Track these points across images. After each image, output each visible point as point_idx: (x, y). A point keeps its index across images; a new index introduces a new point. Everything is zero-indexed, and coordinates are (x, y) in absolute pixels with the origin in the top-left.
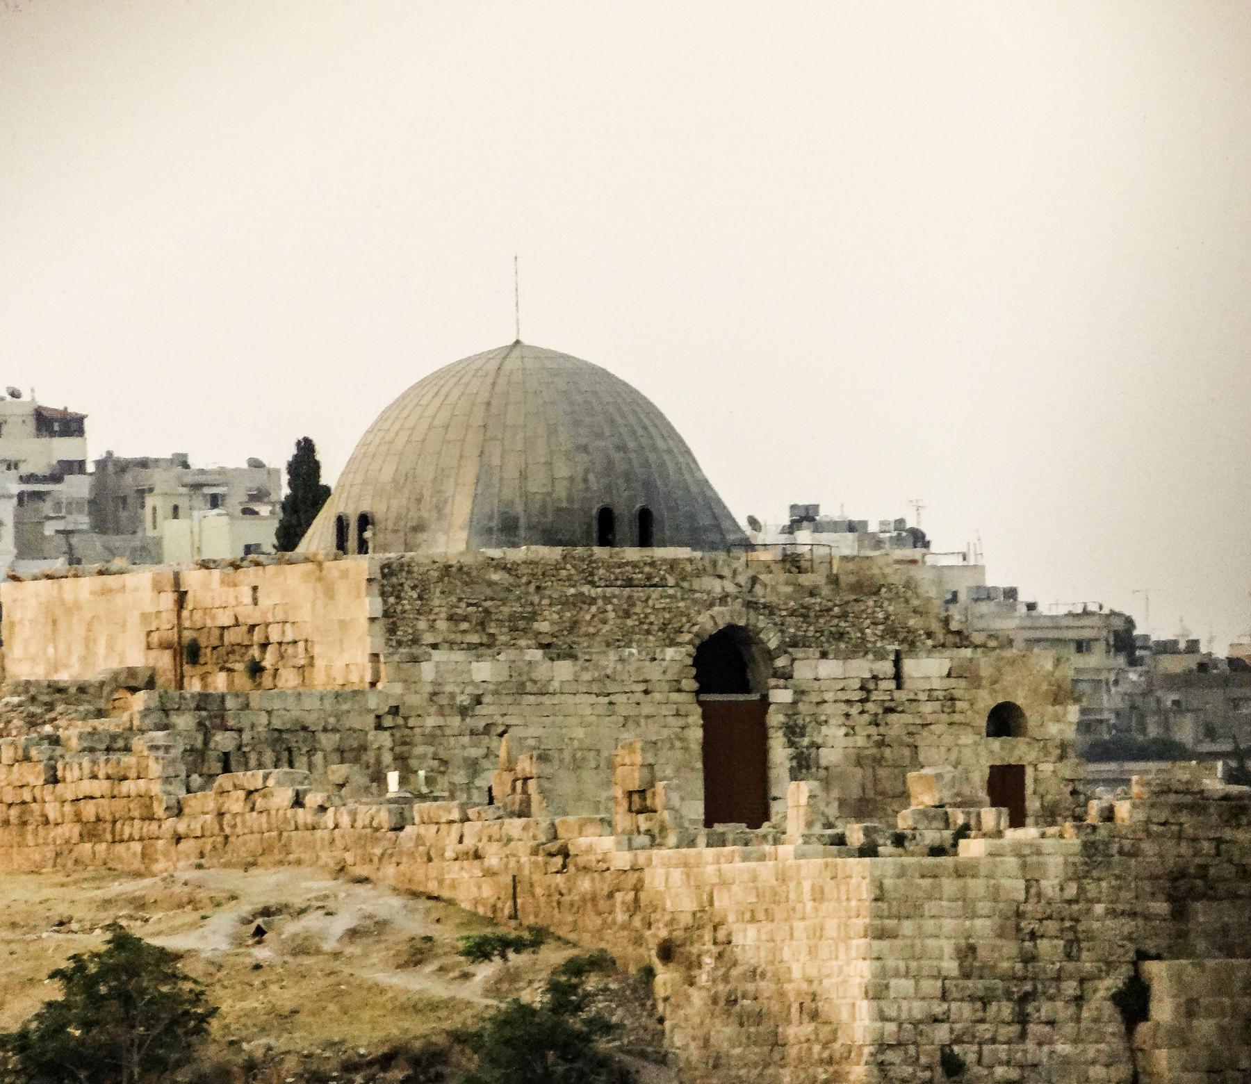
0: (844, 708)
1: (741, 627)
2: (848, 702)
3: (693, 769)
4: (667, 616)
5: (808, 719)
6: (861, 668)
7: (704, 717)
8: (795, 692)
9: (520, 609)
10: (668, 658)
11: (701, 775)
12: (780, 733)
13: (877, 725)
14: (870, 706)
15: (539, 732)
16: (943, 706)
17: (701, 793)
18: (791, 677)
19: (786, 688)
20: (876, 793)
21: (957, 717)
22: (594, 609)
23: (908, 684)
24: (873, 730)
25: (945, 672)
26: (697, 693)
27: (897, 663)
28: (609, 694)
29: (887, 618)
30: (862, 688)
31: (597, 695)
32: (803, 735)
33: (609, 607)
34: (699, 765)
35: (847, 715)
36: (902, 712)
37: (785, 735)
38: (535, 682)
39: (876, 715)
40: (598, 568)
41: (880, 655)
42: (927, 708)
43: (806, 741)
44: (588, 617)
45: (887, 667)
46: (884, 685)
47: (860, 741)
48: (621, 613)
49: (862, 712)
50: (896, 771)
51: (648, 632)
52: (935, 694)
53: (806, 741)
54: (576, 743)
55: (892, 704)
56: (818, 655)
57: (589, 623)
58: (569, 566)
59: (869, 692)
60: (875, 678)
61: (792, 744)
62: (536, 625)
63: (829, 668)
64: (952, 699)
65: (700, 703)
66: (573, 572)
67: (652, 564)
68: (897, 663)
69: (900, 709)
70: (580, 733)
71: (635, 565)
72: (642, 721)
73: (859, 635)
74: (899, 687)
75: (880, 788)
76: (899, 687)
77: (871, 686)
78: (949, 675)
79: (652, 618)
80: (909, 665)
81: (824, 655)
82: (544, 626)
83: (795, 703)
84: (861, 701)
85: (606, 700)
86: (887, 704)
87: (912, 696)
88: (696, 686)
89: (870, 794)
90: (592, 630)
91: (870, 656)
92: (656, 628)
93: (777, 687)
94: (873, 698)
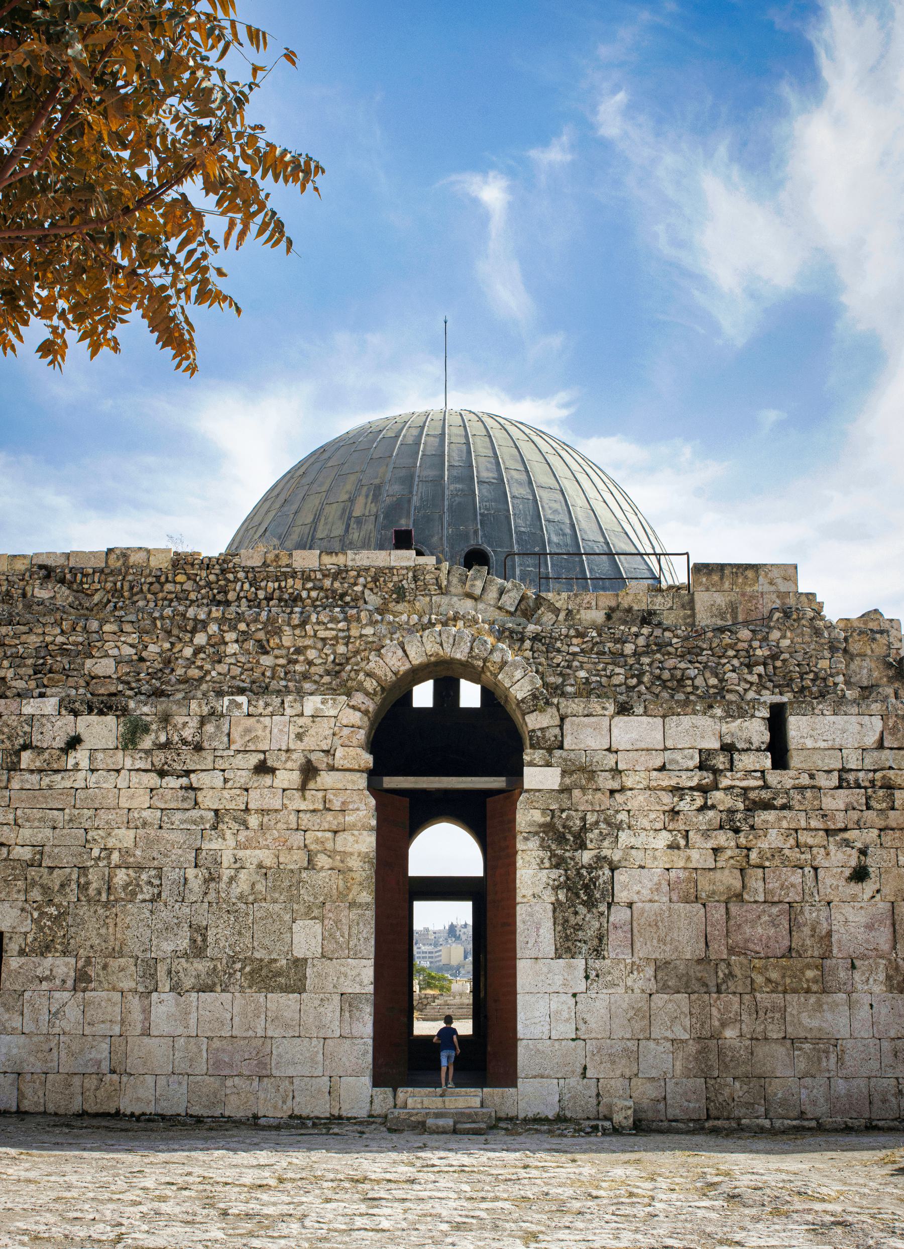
0: (667, 799)
1: (459, 662)
2: (677, 790)
3: (353, 905)
4: (341, 649)
5: (591, 818)
6: (699, 731)
7: (380, 810)
8: (564, 773)
9: (60, 639)
10: (308, 711)
11: (370, 914)
12: (534, 843)
13: (737, 831)
14: (717, 796)
15: (39, 838)
16: (868, 798)
17: (369, 949)
18: (561, 747)
19: (548, 765)
20: (731, 951)
21: (894, 818)
22: (200, 639)
23: (796, 760)
24: (723, 838)
25: (871, 740)
26: (374, 774)
27: (777, 721)
28: (188, 773)
29: (774, 657)
30: (701, 767)
31: (162, 774)
32: (583, 846)
33: (230, 636)
34: (367, 897)
35: (674, 813)
36: (784, 807)
37: (543, 847)
38: (40, 750)
39: (731, 812)
40: (237, 580)
41: (741, 711)
42: (836, 802)
43: (586, 857)
44: (188, 652)
45: (756, 730)
46: (746, 761)
47: (699, 856)
48: (250, 645)
49: (701, 809)
50: (775, 910)
51: (306, 676)
52: (851, 777)
53: (586, 857)
54: (115, 857)
55: (765, 795)
56: (611, 708)
57: (191, 662)
58: (181, 578)
59: (716, 772)
60: (728, 748)
61: (559, 863)
62: (89, 663)
63: (636, 732)
64: (889, 786)
65: (374, 788)
66: (189, 586)
67: (340, 573)
68: (777, 721)
69: (779, 802)
70: (125, 837)
71: (306, 577)
72: (253, 821)
73: (713, 681)
74: (780, 761)
75: (737, 938)
76: (780, 761)
77: (720, 761)
78: (880, 746)
79: (311, 654)
80: (797, 727)
81: (624, 709)
82: (104, 667)
83: (565, 790)
84: (703, 790)
85: (184, 781)
86: (752, 795)
87: (805, 780)
88: (367, 760)
89: (719, 950)
90: (194, 673)
91: (718, 712)
92: (320, 670)
93: (532, 764)
94: (725, 782)
